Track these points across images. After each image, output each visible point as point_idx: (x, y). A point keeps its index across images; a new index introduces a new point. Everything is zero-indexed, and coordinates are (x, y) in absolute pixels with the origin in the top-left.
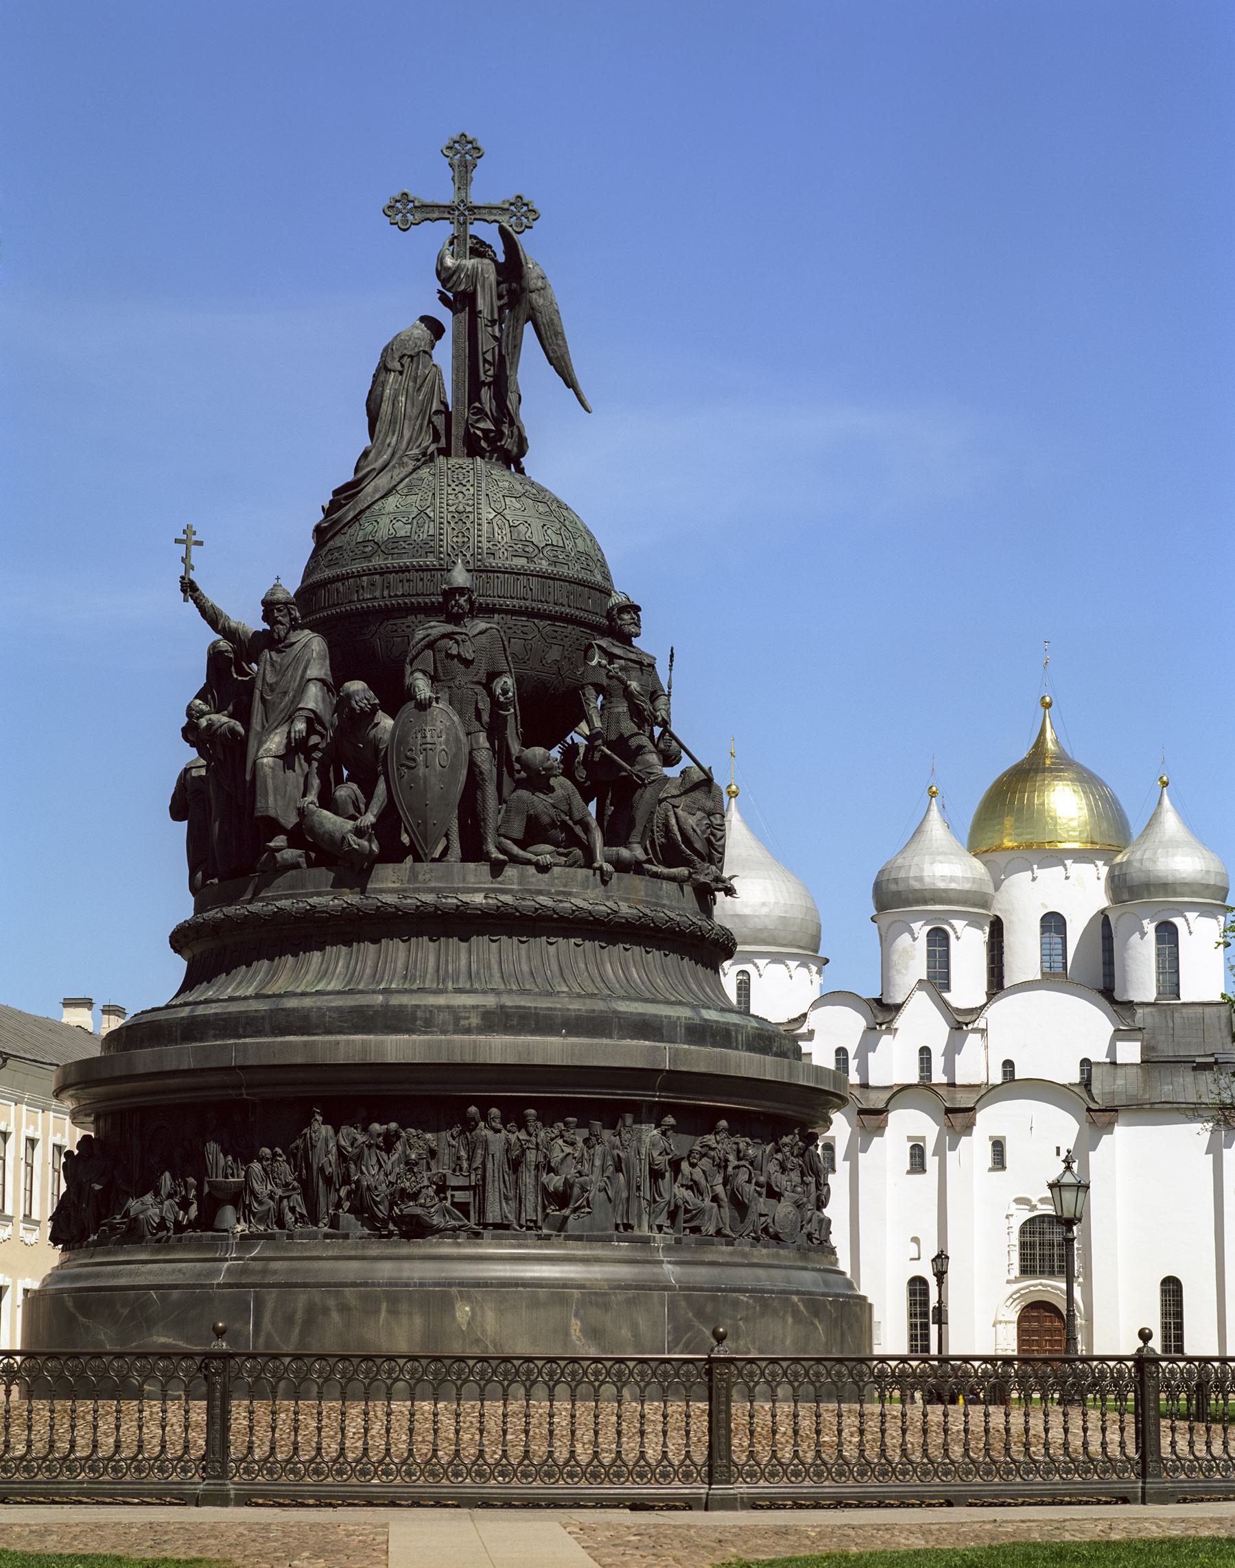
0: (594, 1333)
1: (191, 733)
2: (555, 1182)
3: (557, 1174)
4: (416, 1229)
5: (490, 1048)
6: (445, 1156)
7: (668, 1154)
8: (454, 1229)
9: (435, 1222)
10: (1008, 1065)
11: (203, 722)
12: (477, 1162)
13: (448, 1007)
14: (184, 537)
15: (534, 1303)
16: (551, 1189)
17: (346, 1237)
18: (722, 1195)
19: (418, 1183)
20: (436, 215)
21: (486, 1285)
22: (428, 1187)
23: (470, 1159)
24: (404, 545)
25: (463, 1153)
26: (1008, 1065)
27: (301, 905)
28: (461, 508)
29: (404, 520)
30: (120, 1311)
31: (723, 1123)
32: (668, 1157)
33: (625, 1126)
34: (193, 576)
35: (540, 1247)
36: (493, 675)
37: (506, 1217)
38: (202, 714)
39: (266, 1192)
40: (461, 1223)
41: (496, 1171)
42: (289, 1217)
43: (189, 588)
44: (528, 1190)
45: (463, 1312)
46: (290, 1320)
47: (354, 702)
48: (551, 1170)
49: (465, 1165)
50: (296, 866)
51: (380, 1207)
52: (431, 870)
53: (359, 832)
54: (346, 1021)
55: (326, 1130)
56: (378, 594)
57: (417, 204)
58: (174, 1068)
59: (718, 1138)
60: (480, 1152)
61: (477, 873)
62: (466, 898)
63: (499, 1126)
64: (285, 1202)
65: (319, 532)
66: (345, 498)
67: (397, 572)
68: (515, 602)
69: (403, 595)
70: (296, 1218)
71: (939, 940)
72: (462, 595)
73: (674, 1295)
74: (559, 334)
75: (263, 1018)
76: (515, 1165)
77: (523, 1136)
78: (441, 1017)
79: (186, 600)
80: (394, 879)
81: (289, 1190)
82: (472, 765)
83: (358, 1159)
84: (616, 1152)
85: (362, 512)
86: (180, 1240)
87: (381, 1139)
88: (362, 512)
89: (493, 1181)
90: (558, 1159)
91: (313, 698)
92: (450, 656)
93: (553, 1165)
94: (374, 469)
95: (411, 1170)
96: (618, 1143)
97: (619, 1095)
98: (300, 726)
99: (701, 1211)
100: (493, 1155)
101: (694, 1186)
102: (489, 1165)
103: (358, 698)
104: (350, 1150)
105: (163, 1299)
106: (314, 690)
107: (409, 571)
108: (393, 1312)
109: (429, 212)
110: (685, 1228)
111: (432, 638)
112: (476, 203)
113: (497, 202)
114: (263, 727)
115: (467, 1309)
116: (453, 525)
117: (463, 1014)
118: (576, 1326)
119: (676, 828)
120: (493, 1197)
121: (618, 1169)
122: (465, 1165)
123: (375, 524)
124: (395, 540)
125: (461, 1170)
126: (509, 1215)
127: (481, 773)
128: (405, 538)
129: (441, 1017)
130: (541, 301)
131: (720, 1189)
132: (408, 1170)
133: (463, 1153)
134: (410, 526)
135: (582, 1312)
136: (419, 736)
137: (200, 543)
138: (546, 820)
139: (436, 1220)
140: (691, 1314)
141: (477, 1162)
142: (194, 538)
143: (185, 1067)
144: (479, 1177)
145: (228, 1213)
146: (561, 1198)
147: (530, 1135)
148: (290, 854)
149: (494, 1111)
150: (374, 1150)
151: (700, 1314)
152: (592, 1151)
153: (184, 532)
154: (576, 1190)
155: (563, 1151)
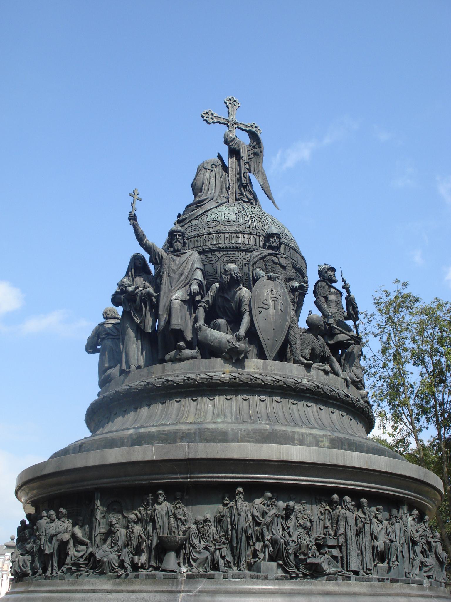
2: (380, 544)
5: (352, 457)
8: (335, 574)
13: (311, 434)
16: (379, 549)
24: (233, 223)
27: (202, 376)
28: (258, 213)
29: (232, 214)
33: (404, 513)
41: (353, 536)
43: (133, 218)
47: (233, 274)
49: (332, 532)
52: (275, 365)
54: (252, 438)
56: (221, 242)
57: (215, 115)
60: (342, 523)
66: (196, 207)
69: (235, 243)
75: (195, 433)
78: (308, 439)
80: (254, 367)
85: (206, 211)
89: (352, 543)
90: (378, 530)
92: (274, 263)
93: (376, 535)
94: (208, 198)
98: (195, 287)
102: (349, 533)
107: (238, 233)
111: (265, 255)
114: (169, 290)
117: (320, 439)
123: (216, 215)
124: (229, 221)
125: (330, 535)
128: (234, 221)
129: (309, 439)
133: (328, 524)
134: (235, 216)
136: (270, 293)
138: (318, 352)
141: (341, 531)
143: (149, 458)
147: (365, 514)
148: (188, 352)
149: (347, 498)
150: (280, 519)
152: (393, 527)
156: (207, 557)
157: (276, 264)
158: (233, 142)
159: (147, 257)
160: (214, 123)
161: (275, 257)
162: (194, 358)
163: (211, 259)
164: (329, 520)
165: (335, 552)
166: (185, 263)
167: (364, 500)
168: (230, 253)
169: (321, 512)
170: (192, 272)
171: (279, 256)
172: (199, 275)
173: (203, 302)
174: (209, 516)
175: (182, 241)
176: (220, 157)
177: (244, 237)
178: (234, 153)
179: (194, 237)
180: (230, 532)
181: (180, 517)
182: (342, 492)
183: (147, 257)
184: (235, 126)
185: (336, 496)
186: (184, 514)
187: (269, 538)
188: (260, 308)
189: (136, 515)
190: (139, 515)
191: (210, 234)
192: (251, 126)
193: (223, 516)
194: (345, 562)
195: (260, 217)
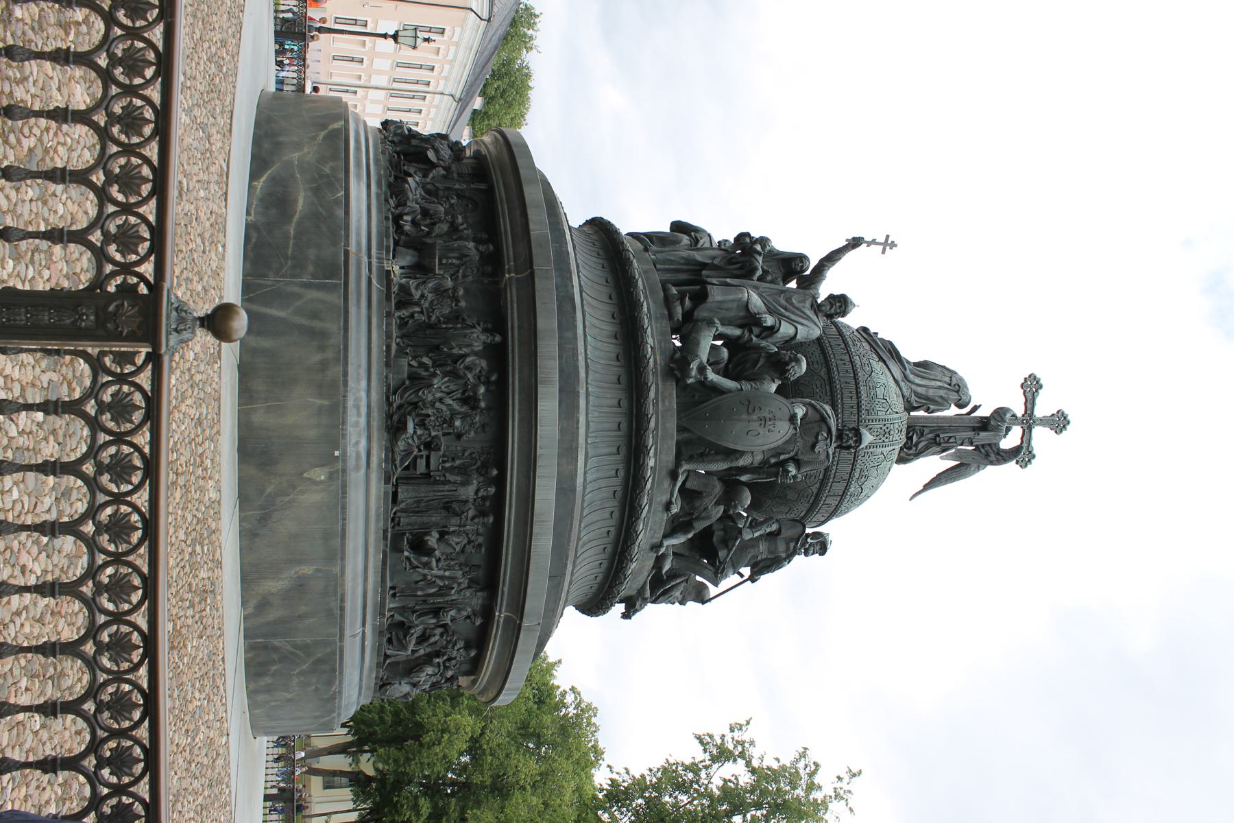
0: (301, 586)
1: (742, 238)
2: (432, 540)
3: (439, 540)
4: (394, 428)
6: (458, 446)
7: (452, 621)
8: (393, 461)
9: (399, 443)
11: (758, 248)
12: (450, 477)
14: (889, 242)
15: (327, 537)
16: (427, 538)
17: (388, 364)
18: (417, 655)
19: (434, 427)
20: (1029, 406)
21: (344, 493)
22: (430, 435)
23: (451, 470)
25: (458, 462)
27: (646, 321)
28: (892, 432)
30: (328, 166)
31: (473, 653)
32: (449, 622)
34: (864, 245)
35: (377, 533)
36: (798, 463)
37: (403, 502)
38: (763, 247)
39: (426, 292)
40: (398, 465)
41: (442, 494)
42: (404, 313)
43: (855, 243)
44: (425, 518)
45: (321, 475)
46: (315, 315)
47: (793, 364)
48: (442, 535)
49: (447, 465)
50: (671, 316)
51: (413, 395)
53: (702, 369)
55: (478, 347)
59: (461, 650)
60: (459, 479)
61: (669, 457)
62: (652, 453)
63: (480, 494)
64: (417, 309)
65: (865, 330)
66: (889, 350)
67: (857, 389)
68: (833, 472)
70: (404, 318)
72: (856, 442)
73: (336, 643)
74: (954, 480)
76: (448, 507)
77: (471, 513)
79: (847, 240)
81: (428, 312)
82: (742, 453)
83: (454, 375)
84: (455, 586)
86: (387, 218)
87: (471, 394)
88: (885, 362)
89: (435, 491)
91: (786, 329)
92: (817, 435)
94: (906, 369)
95: (445, 421)
96: (463, 586)
97: (505, 587)
98: (769, 321)
99: (405, 648)
100: (456, 490)
101: (423, 639)
102: (447, 487)
103: (796, 367)
104: (462, 366)
106: (791, 331)
107: (857, 398)
108: (320, 411)
109: (1030, 403)
110: (391, 633)
112: (1033, 430)
113: (1033, 443)
115: (323, 477)
116: (884, 428)
118: (307, 570)
119: (673, 583)
120: (424, 491)
121: (441, 588)
122: (447, 465)
125: (444, 462)
126: (404, 504)
127: (737, 459)
130: (972, 469)
131: (422, 652)
132: (445, 419)
133: (458, 462)
135: (320, 575)
136: (771, 416)
137: (883, 252)
138: (697, 504)
139: (401, 445)
140: (319, 655)
141: (450, 477)
142: (888, 248)
143: (532, 226)
144: (438, 478)
145: (408, 258)
146: (419, 546)
148: (679, 311)
149: (492, 490)
151: (320, 661)
153: (893, 242)
154: (425, 559)
155: (457, 544)
156: (411, 295)
157: (817, 437)
158: (999, 419)
159: (808, 272)
160: (1025, 392)
161: (825, 435)
162: (671, 316)
163: (815, 363)
164: (462, 464)
165: (421, 464)
166: (802, 314)
167: (491, 519)
168: (828, 387)
169: (474, 453)
170: (791, 322)
171: (828, 441)
173: (750, 335)
174: (463, 304)
175: (833, 311)
176: (975, 408)
177: (852, 407)
178: (984, 425)
179: (844, 342)
180: (444, 326)
181: (461, 271)
182: (500, 482)
183: (808, 272)
184: (1025, 427)
185: (495, 472)
187: (438, 372)
188: (747, 403)
189: (462, 224)
190: (462, 227)
191: (851, 361)
192: (1030, 452)
193: (463, 319)
194: (410, 481)
195: (887, 435)
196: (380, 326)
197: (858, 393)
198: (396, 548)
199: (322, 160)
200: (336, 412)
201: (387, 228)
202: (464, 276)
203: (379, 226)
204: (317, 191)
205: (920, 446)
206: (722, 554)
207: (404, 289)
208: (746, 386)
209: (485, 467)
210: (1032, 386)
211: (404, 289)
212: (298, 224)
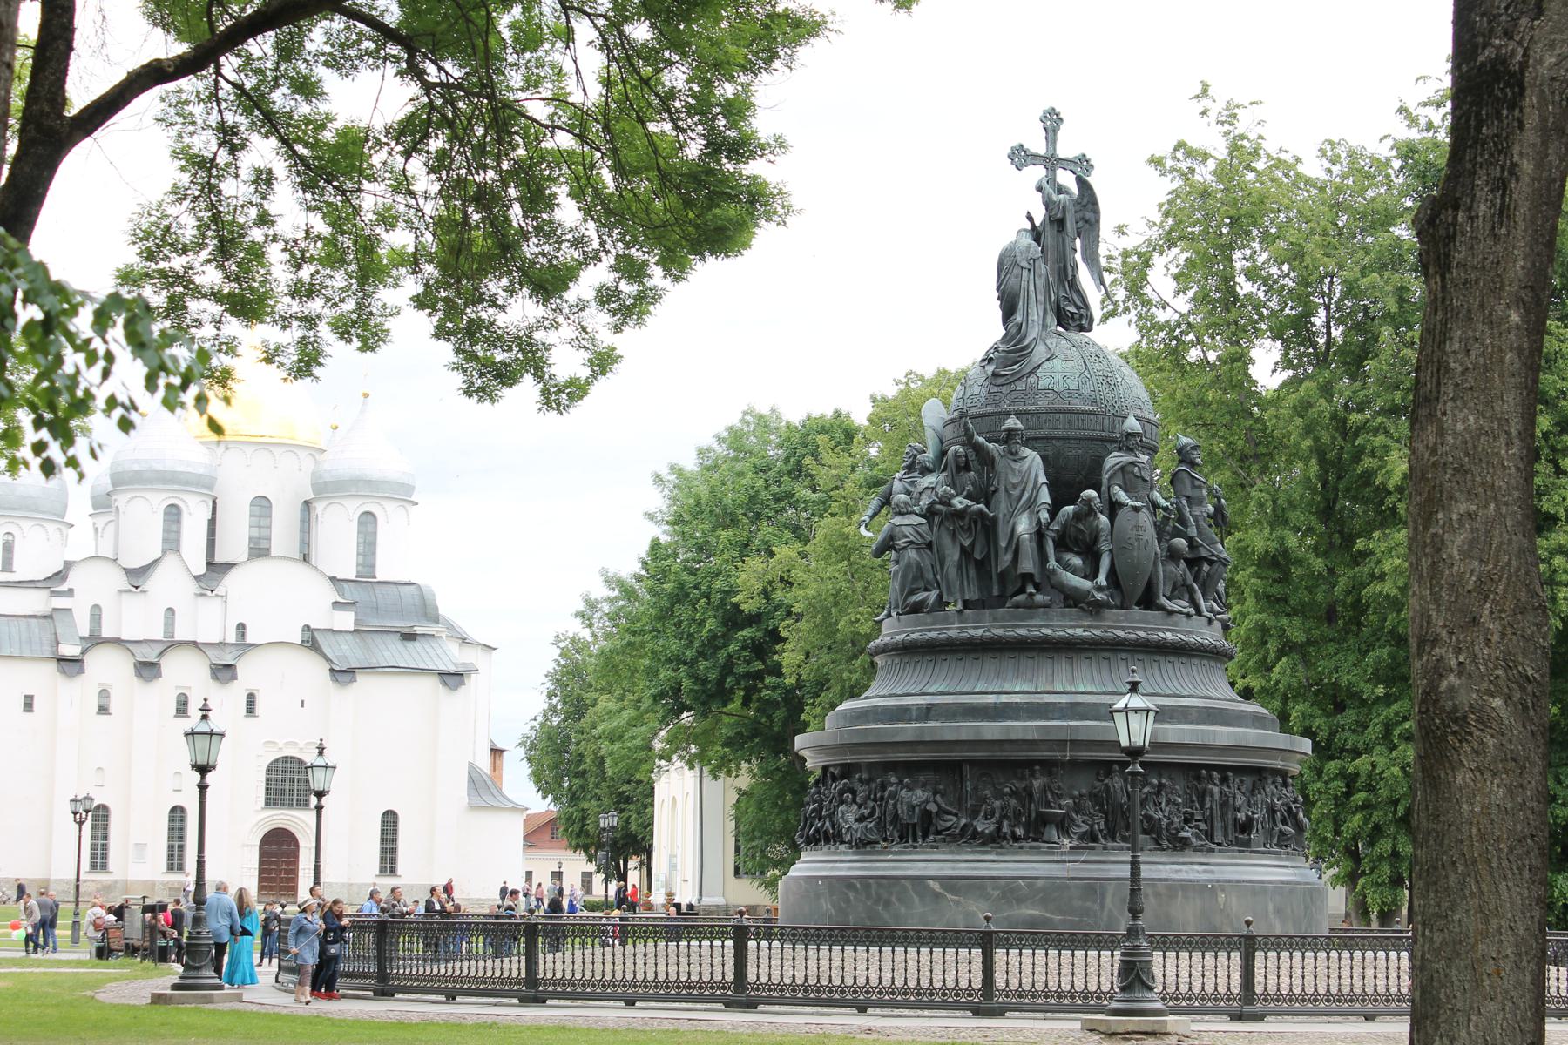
2: (1241, 816)
4: (1181, 845)
10: (241, 627)
26: (241, 627)
53: (1100, 589)
58: (1020, 737)
60: (1208, 799)
71: (173, 514)
86: (1021, 847)
98: (1044, 515)
105: (1029, 886)
106: (1045, 489)
109: (1034, 158)
112: (1061, 156)
113: (1071, 156)
120: (1218, 824)
141: (1208, 806)
146: (1246, 827)
156: (1086, 833)
172: (1045, 497)
182: (1210, 767)
186: (1059, 788)
196: (1115, 855)
197: (1078, 412)
198: (1247, 843)
199: (987, 897)
200: (1187, 887)
201: (1031, 847)
202: (1059, 788)
203: (1027, 853)
204: (1020, 901)
205: (1079, 303)
206: (1204, 553)
207: (1082, 837)
208: (1104, 546)
209: (1198, 778)
210: (1020, 157)
211: (1082, 837)
212: (1052, 913)
